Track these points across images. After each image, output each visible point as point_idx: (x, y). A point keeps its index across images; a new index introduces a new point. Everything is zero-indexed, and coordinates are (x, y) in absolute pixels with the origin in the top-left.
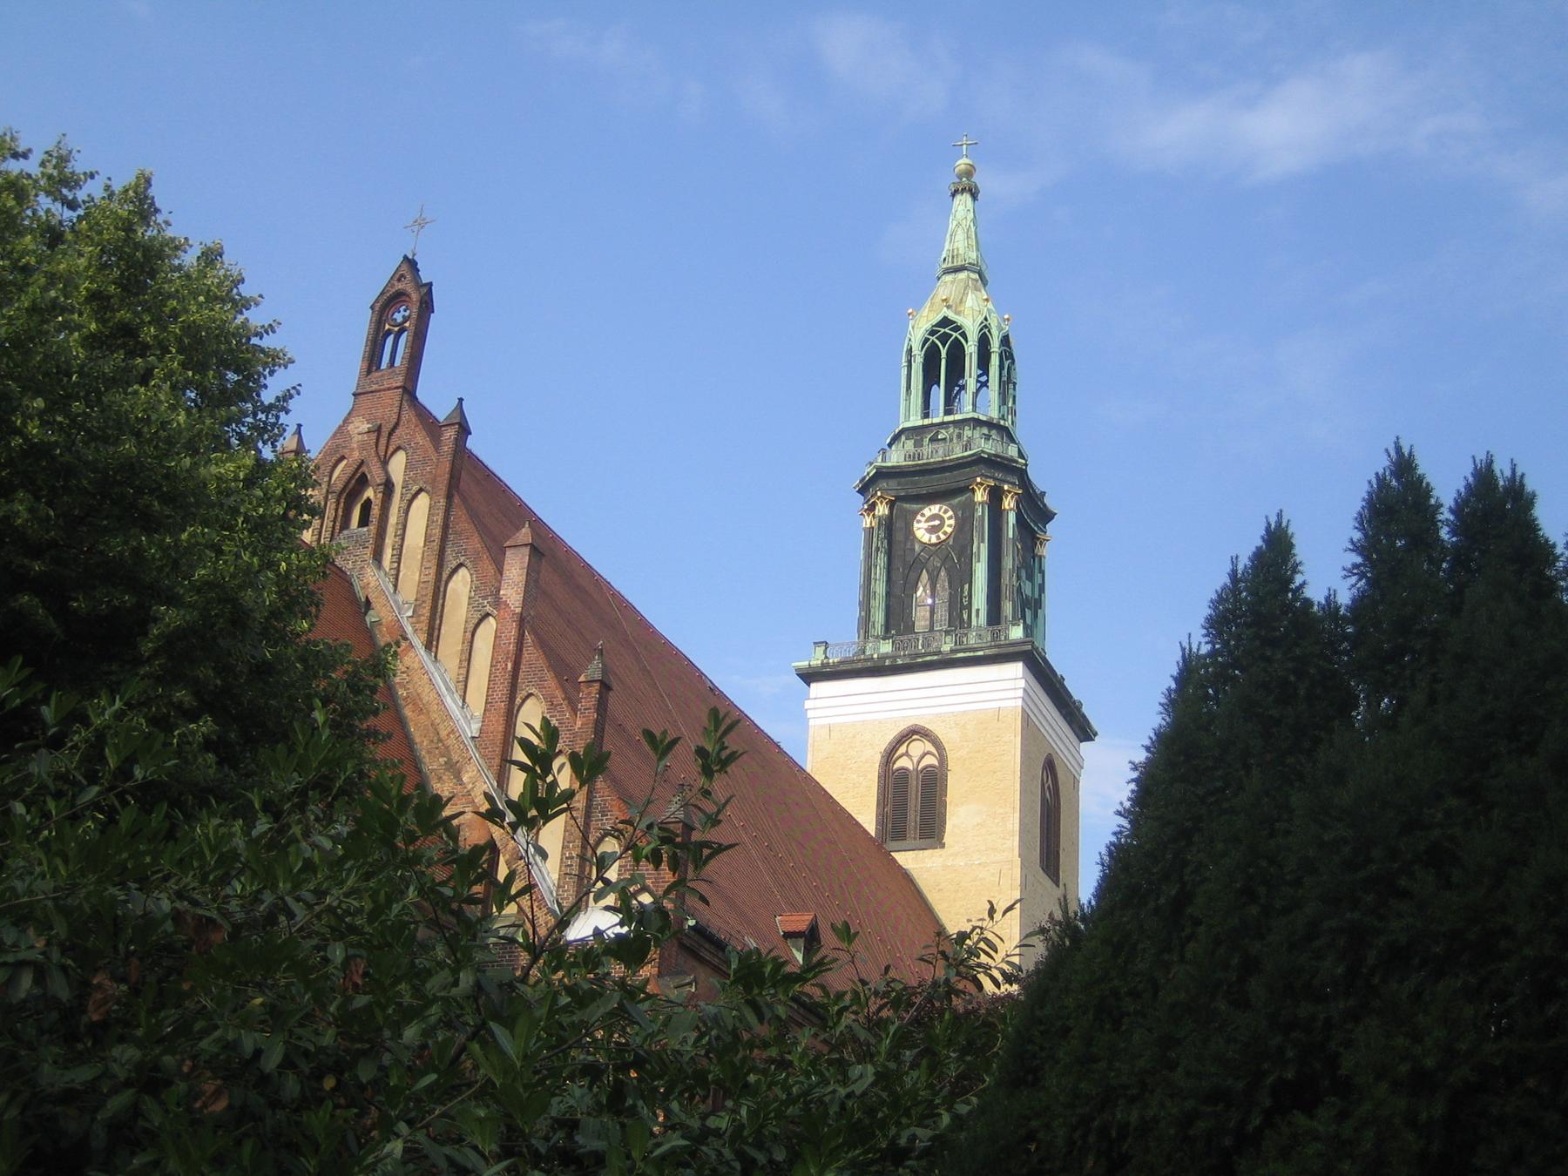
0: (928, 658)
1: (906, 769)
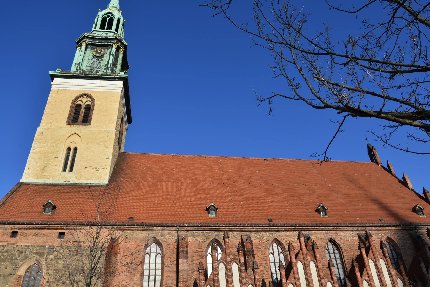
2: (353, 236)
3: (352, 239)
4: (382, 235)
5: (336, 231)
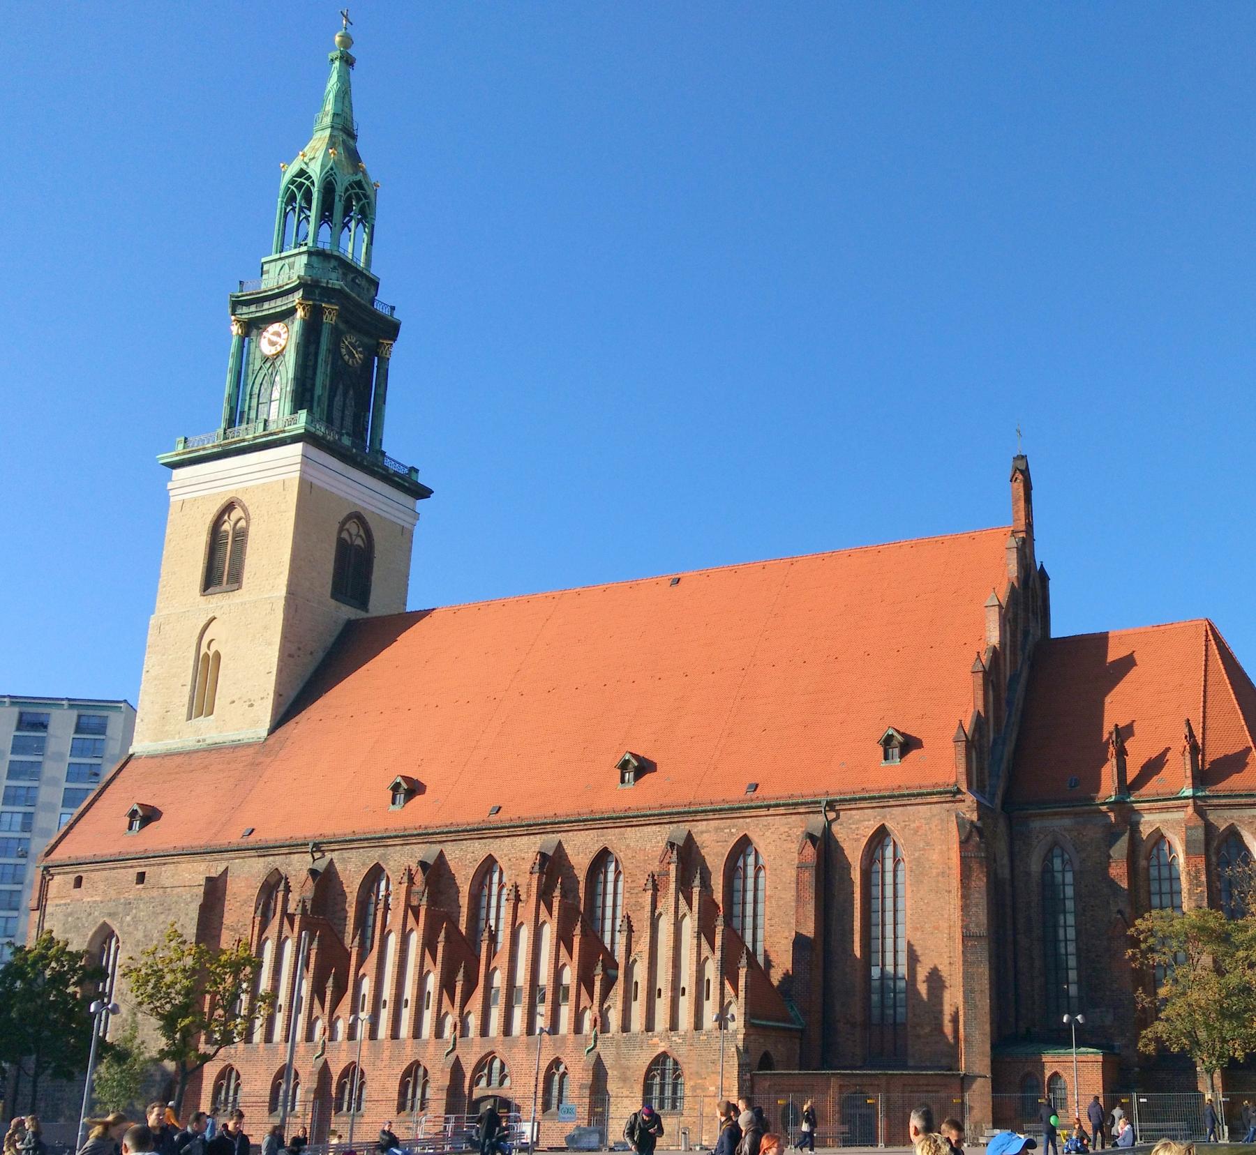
0: (381, 471)
1: (346, 541)
2: (659, 838)
3: (654, 847)
4: (732, 830)
5: (623, 829)
